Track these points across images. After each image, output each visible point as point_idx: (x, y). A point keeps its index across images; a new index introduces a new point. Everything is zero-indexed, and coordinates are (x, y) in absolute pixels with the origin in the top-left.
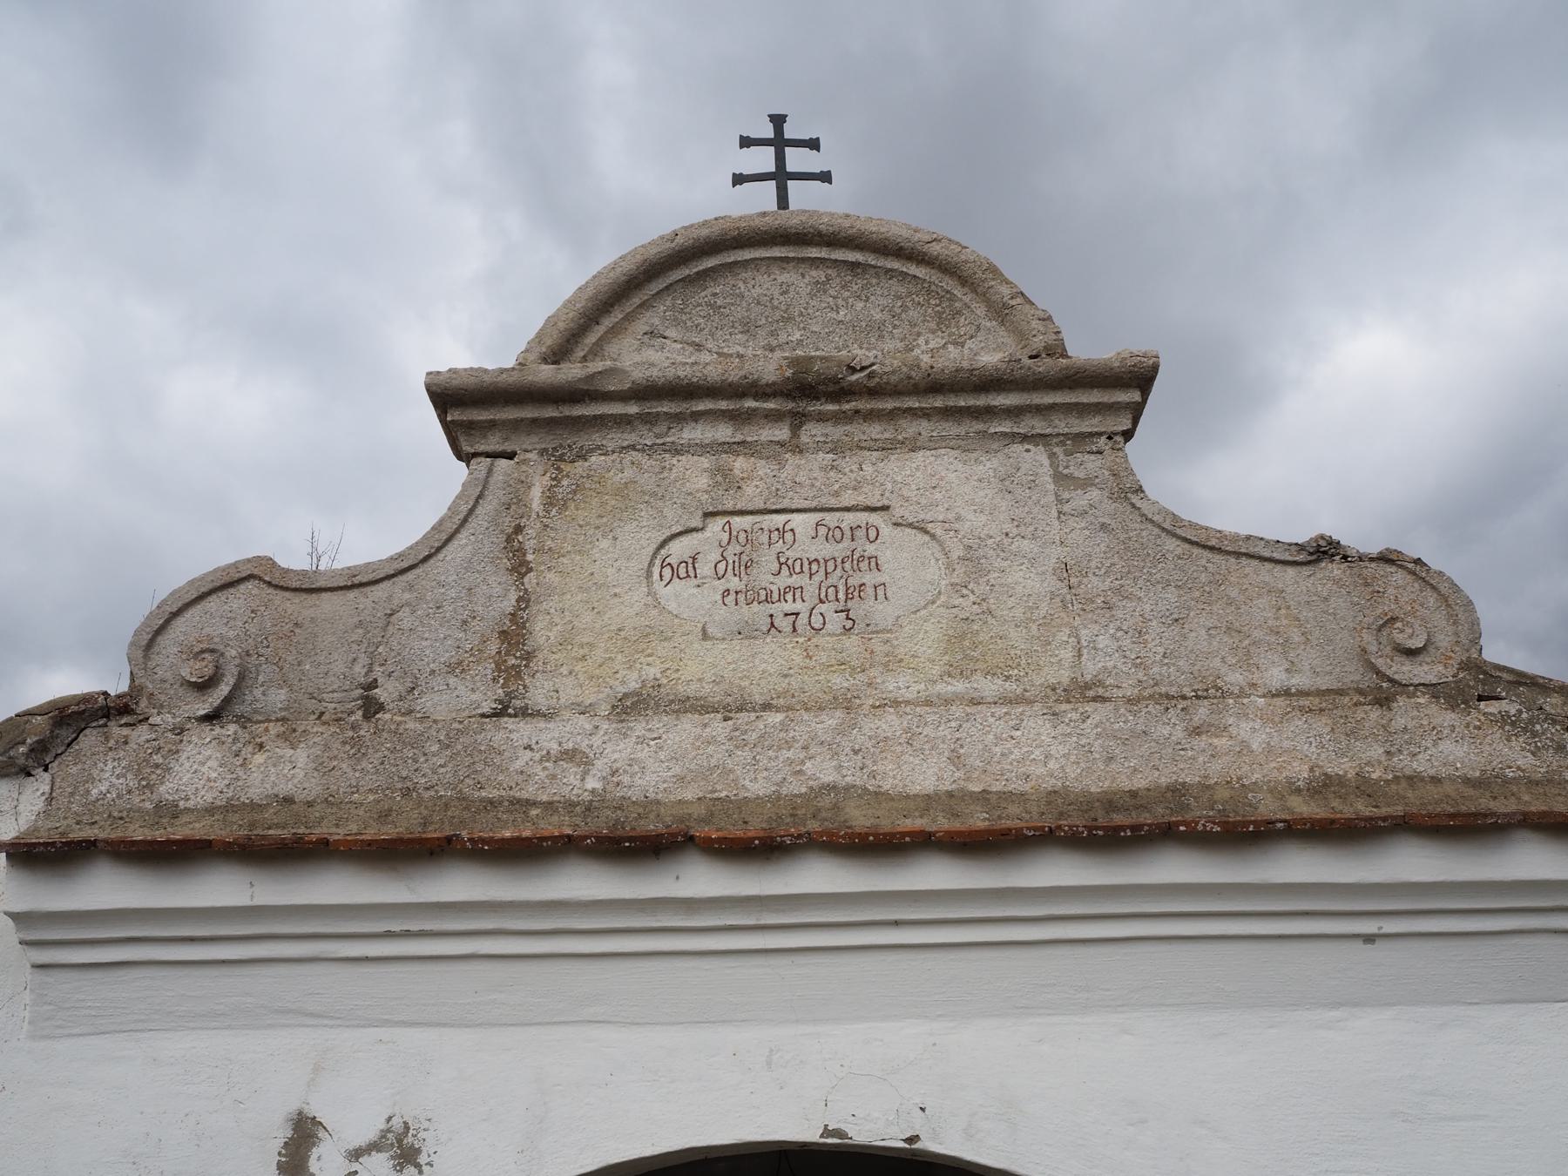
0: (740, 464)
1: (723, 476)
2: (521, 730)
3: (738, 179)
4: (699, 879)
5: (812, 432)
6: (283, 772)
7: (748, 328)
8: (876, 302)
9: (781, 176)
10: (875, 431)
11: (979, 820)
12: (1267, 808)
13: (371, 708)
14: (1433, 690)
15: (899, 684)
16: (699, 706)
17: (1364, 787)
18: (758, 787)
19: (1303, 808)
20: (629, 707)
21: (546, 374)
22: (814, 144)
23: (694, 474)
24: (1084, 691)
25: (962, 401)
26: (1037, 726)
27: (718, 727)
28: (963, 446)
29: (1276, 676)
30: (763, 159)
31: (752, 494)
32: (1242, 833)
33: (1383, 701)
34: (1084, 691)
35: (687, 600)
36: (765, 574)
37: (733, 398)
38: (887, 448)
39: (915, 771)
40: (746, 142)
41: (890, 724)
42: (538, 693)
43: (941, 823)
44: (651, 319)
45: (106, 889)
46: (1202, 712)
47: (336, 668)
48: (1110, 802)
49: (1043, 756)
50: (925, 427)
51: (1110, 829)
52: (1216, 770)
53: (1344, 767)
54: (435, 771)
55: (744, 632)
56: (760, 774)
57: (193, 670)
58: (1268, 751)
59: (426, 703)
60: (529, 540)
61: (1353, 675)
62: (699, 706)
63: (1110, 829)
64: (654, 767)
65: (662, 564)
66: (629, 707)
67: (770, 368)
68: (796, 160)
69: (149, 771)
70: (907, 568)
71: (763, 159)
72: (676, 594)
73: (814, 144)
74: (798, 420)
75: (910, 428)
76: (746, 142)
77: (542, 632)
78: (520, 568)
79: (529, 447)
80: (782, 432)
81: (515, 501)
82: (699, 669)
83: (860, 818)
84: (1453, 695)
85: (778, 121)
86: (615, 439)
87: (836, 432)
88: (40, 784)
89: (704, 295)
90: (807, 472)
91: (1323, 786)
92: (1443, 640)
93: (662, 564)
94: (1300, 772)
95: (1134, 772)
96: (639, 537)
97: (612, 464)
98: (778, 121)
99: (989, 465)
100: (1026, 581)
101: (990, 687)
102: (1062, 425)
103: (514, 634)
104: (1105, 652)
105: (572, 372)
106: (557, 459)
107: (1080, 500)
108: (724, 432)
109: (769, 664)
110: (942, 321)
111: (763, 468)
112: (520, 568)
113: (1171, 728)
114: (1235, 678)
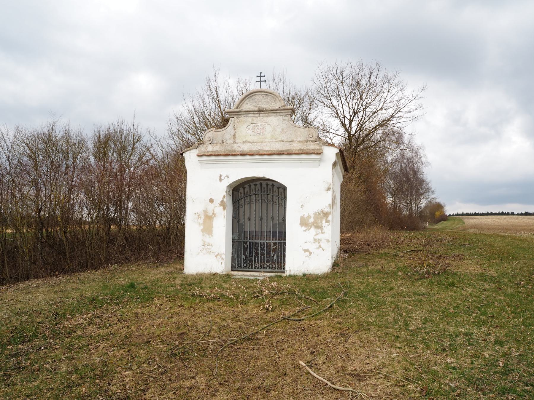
0: (254, 118)
1: (253, 120)
2: (235, 145)
3: (256, 82)
4: (248, 157)
5: (261, 115)
6: (217, 148)
7: (256, 102)
8: (268, 99)
9: (261, 81)
10: (267, 115)
11: (270, 153)
12: (294, 152)
13: (223, 142)
14: (312, 141)
15: (267, 140)
16: (250, 142)
17: (303, 150)
18: (254, 149)
19: (297, 152)
20: (244, 142)
21: (236, 110)
22: (264, 76)
23: (250, 119)
24: (282, 141)
25: (274, 111)
26: (277, 144)
27: (251, 144)
28: (275, 116)
29: (299, 139)
30: (259, 79)
31: (255, 122)
32: (290, 153)
33: (307, 142)
34: (282, 141)
35: (250, 132)
36: (256, 130)
37: (253, 112)
38: (268, 116)
39: (266, 148)
40: (257, 76)
41: (265, 144)
42: (237, 141)
43: (267, 153)
44: (247, 101)
45: (205, 158)
46: (291, 143)
47: (220, 139)
48: (281, 151)
49: (277, 147)
50: (271, 114)
51: (280, 153)
52: (291, 148)
53: (302, 148)
54: (229, 148)
55: (254, 135)
56: (254, 148)
57: (209, 140)
58: (296, 146)
59: (227, 142)
60: (235, 126)
61: (306, 139)
62: (250, 142)
63: (280, 153)
64: (246, 148)
65: (247, 129)
66: (244, 142)
67: (256, 109)
68: (263, 79)
69: (206, 148)
70: (268, 129)
71: (259, 79)
72: (248, 131)
73: (264, 76)
74: (259, 114)
75: (270, 114)
76: (257, 76)
77: (237, 135)
78: (235, 129)
79: (235, 117)
80: (258, 115)
81: (234, 123)
82: (250, 139)
83: (261, 152)
84: (313, 141)
85: (261, 73)
86: (243, 116)
87: (263, 115)
88: (198, 149)
89: (251, 98)
90: (260, 119)
91: (300, 149)
92: (314, 136)
93: (247, 129)
94: (298, 148)
95: (284, 148)
96: (245, 126)
97: (243, 118)
98: (261, 73)
99: (277, 118)
100: (279, 130)
101: (274, 140)
102: (284, 114)
103: (234, 136)
104: (284, 137)
105: (238, 110)
106: (238, 118)
107: (285, 122)
108: (253, 115)
109: (255, 138)
110: (275, 101)
111: (256, 119)
112: (235, 129)
113: (288, 144)
114: (295, 140)
